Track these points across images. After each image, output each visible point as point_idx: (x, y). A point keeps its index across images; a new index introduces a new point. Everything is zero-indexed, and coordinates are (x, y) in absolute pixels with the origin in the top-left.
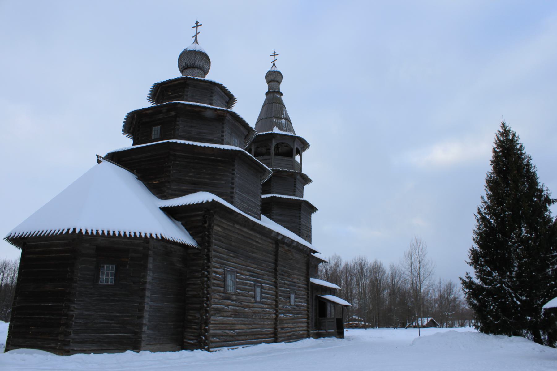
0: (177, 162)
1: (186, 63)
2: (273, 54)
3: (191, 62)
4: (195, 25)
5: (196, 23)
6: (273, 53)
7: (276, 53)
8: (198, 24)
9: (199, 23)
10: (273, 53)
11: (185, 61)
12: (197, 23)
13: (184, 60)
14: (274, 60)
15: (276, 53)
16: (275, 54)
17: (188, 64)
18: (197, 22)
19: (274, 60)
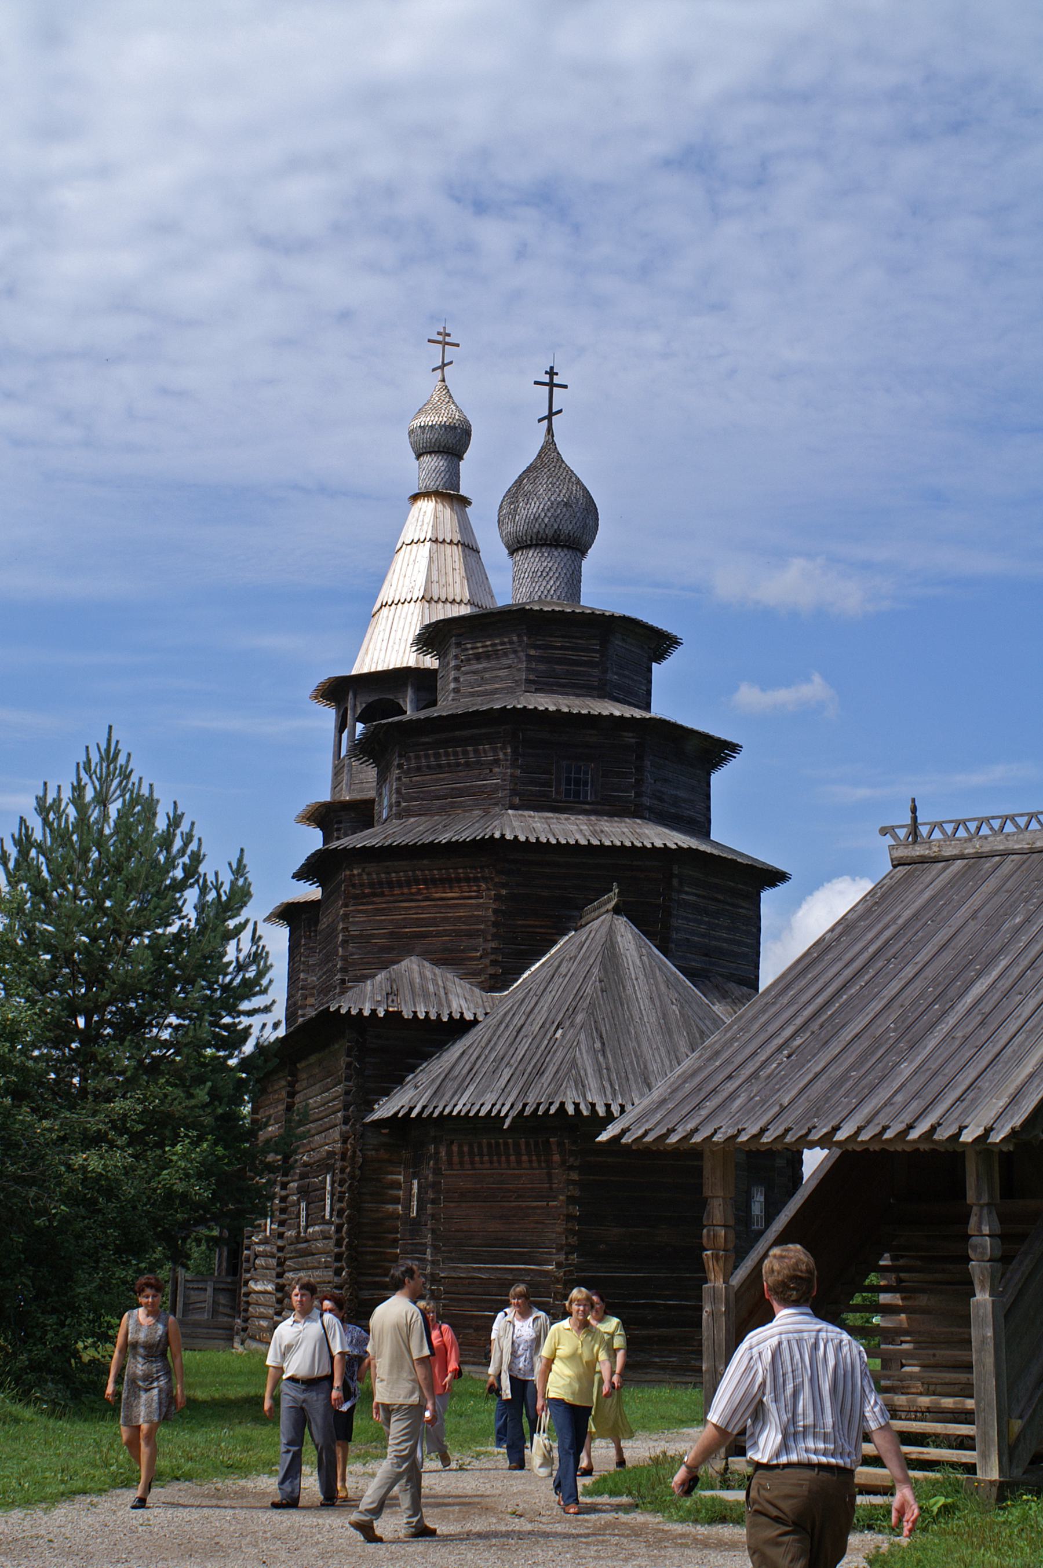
0: (684, 896)
1: (555, 531)
2: (440, 338)
3: (571, 534)
4: (546, 379)
5: (546, 373)
6: (439, 333)
7: (449, 335)
8: (557, 380)
9: (557, 374)
10: (439, 333)
11: (556, 527)
12: (551, 373)
13: (552, 520)
14: (444, 365)
15: (449, 335)
16: (448, 339)
17: (562, 538)
18: (552, 368)
19: (444, 365)
